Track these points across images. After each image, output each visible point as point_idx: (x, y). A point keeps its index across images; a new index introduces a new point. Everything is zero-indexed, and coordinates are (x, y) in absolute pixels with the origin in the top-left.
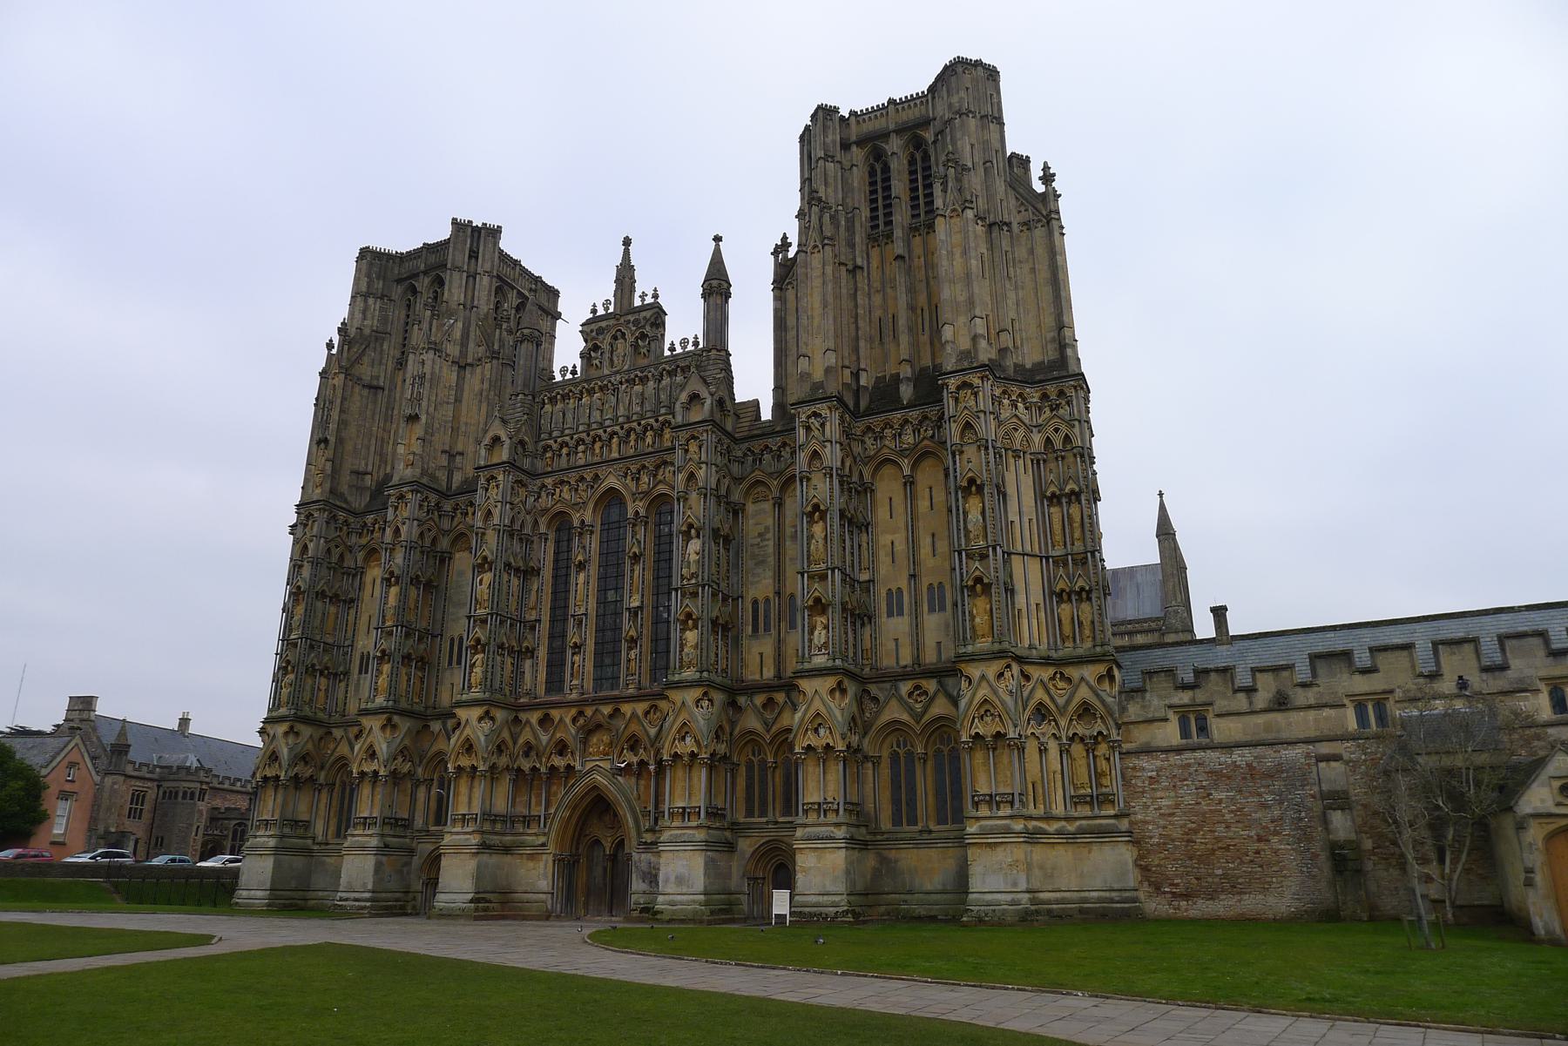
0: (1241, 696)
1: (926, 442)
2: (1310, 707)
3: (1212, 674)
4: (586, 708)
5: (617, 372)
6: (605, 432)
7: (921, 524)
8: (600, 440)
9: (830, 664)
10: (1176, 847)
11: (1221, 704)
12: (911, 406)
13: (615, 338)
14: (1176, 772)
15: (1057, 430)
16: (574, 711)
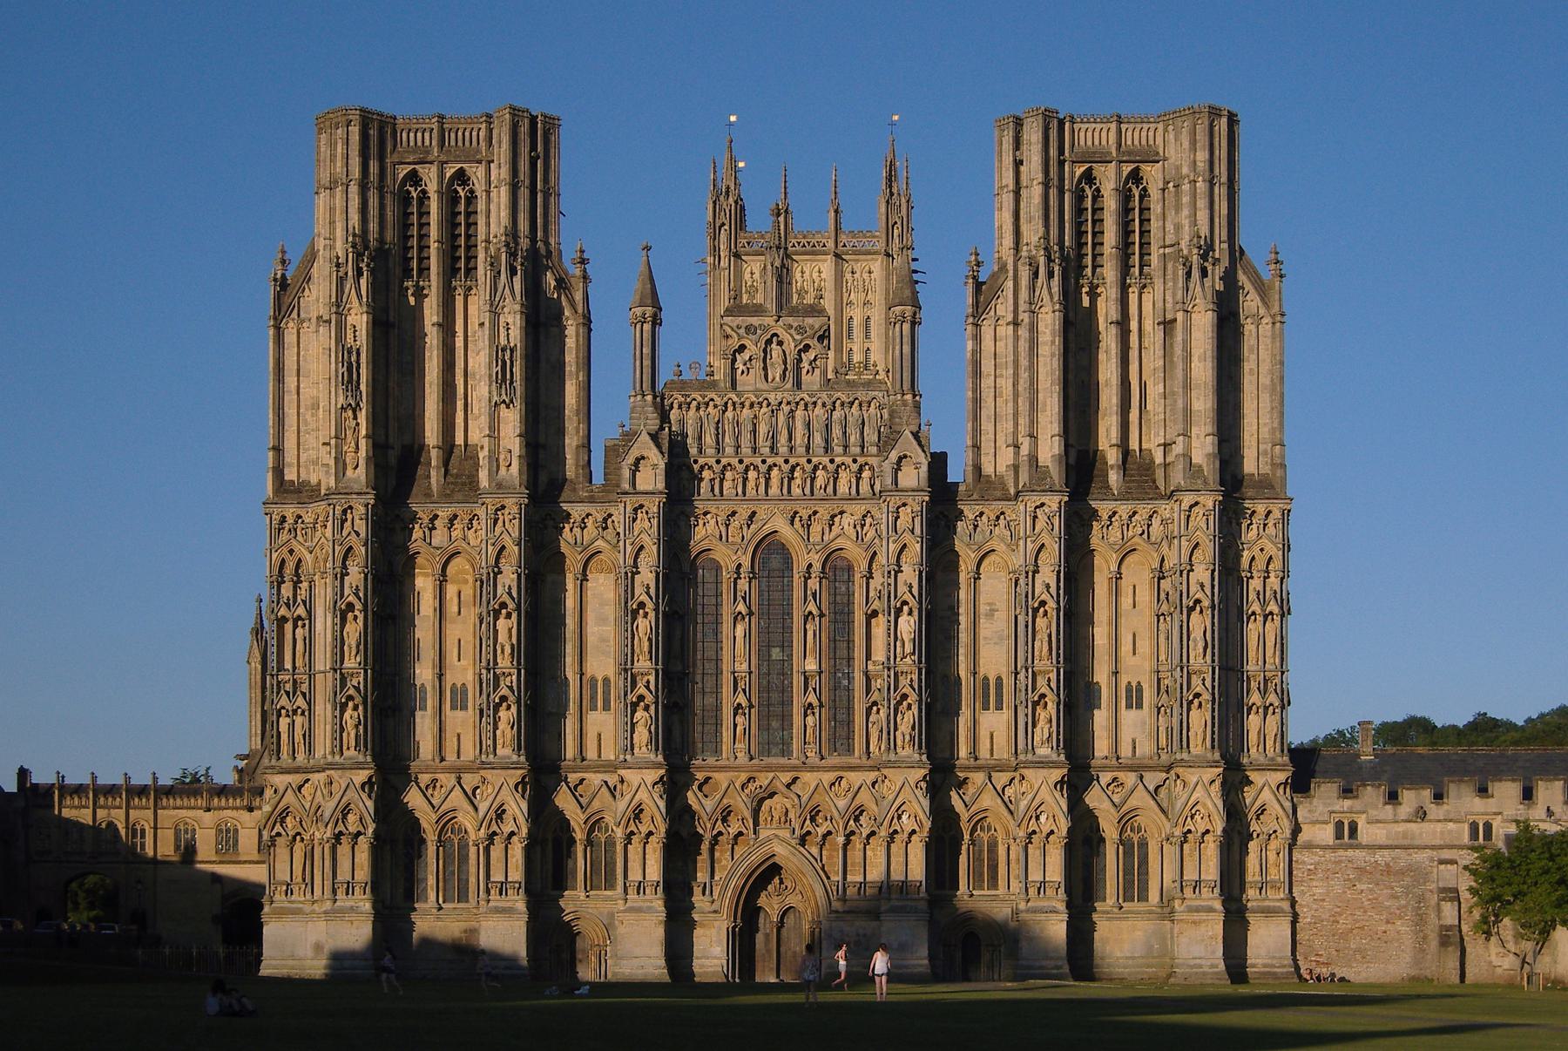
0: (1389, 807)
1: (1137, 539)
2: (1439, 821)
3: (1369, 788)
4: (763, 774)
5: (776, 389)
6: (764, 462)
7: (1123, 621)
8: (756, 468)
9: (1054, 757)
10: (1323, 926)
11: (1373, 813)
12: (1124, 497)
13: (769, 342)
14: (1330, 866)
15: (1262, 550)
16: (744, 777)
